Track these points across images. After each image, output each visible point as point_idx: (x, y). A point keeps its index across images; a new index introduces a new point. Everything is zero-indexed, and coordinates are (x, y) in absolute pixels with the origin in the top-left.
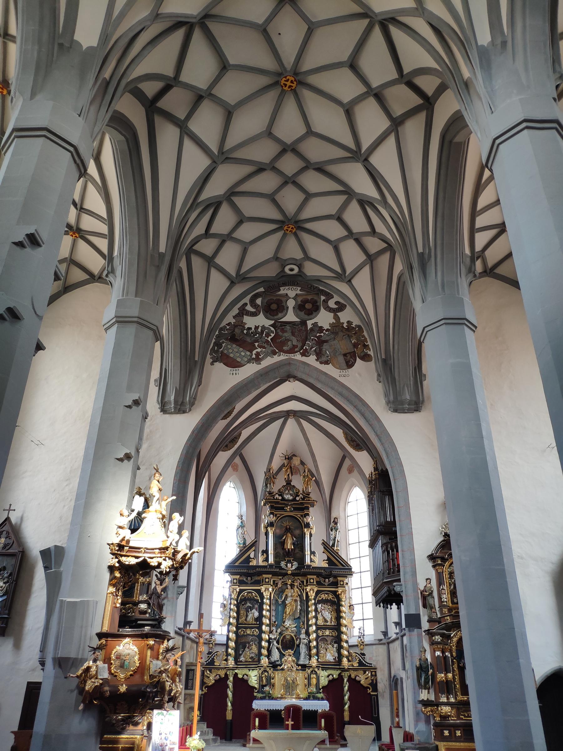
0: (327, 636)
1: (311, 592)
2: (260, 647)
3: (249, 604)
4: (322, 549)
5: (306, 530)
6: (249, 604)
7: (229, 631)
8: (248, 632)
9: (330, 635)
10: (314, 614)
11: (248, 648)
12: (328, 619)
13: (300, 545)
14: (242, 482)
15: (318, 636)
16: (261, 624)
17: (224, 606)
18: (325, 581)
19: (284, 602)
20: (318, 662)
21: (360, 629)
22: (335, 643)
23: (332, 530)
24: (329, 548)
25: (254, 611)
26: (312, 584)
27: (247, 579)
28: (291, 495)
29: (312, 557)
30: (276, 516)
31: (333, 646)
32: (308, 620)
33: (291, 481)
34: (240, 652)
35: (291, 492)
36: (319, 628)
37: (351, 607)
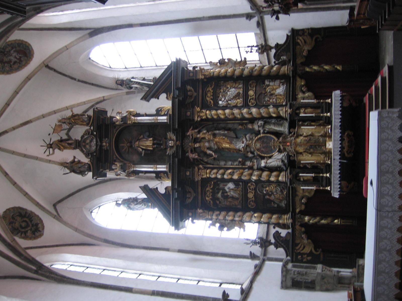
0: (255, 93)
1: (201, 114)
2: (269, 182)
3: (219, 195)
4: (153, 100)
5: (129, 122)
6: (219, 195)
7: (250, 221)
8: (251, 195)
9: (254, 88)
10: (227, 111)
11: (270, 195)
12: (237, 92)
13: (152, 129)
14: (91, 198)
15: (256, 106)
16: (240, 180)
17: (221, 228)
18: (191, 96)
19: (215, 151)
20: (286, 105)
21: (247, 52)
22: (264, 83)
23: (131, 88)
24: (153, 90)
25: (226, 188)
26: (193, 114)
27: (189, 198)
28: (91, 141)
29: (162, 114)
30: (115, 161)
31: (268, 86)
32: (235, 119)
33: (76, 141)
34: (276, 206)
35: (88, 141)
36: (246, 105)
37: (222, 62)
